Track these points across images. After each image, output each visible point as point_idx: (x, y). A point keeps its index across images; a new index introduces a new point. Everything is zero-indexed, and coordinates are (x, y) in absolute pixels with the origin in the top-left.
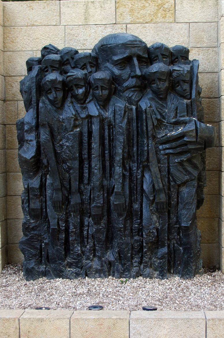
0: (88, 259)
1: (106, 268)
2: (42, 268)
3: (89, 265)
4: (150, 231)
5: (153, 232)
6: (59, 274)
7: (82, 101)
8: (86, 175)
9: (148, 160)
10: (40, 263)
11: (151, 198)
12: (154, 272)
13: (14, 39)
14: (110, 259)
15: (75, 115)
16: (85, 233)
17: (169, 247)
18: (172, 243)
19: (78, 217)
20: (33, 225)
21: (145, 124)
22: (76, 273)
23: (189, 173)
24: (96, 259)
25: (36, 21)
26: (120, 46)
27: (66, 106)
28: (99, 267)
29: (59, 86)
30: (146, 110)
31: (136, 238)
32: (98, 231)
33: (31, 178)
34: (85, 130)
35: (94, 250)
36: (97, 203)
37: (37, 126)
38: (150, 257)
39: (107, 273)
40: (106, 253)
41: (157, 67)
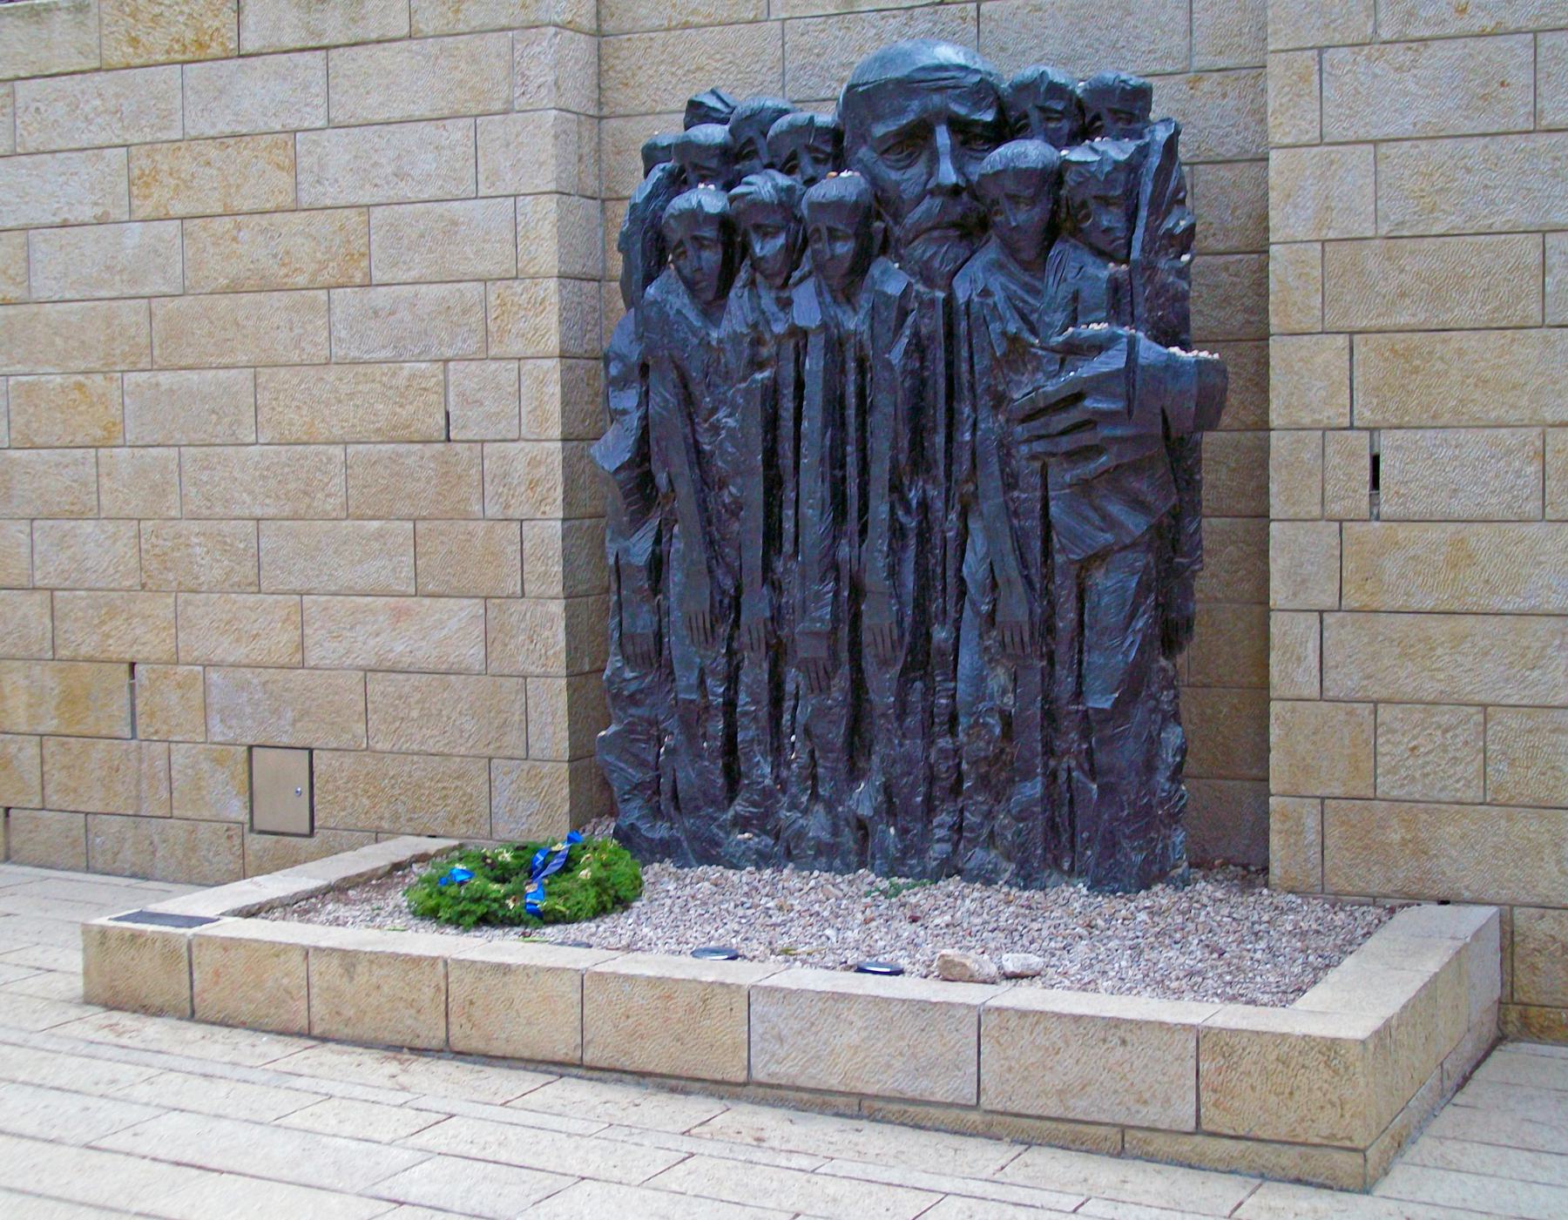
0: (793, 806)
1: (848, 839)
2: (661, 831)
3: (796, 826)
4: (976, 721)
5: (985, 725)
7: (783, 277)
8: (789, 526)
11: (984, 608)
12: (1004, 864)
13: (629, 74)
14: (860, 812)
15: (755, 326)
18: (1065, 766)
19: (765, 666)
20: (633, 687)
21: (965, 353)
22: (758, 852)
23: (1110, 523)
24: (819, 808)
25: (694, 12)
26: (890, 87)
27: (732, 294)
28: (825, 836)
29: (709, 232)
30: (968, 303)
31: (944, 742)
32: (820, 712)
33: (623, 533)
34: (789, 371)
35: (814, 777)
36: (814, 620)
37: (644, 369)
38: (990, 812)
39: (853, 858)
40: (852, 790)
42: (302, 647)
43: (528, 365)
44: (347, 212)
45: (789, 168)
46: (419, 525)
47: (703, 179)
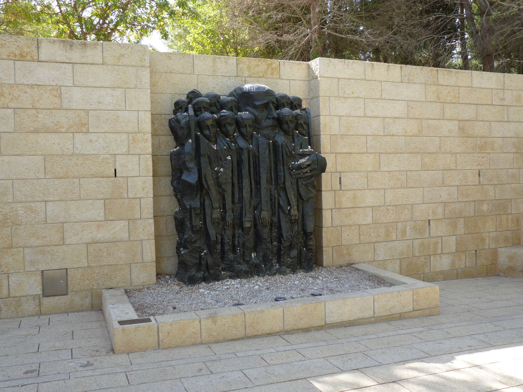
0: (239, 263)
6: (217, 278)
9: (284, 183)
10: (199, 270)
16: (236, 242)
17: (297, 248)
29: (215, 124)
41: (286, 110)
42: (63, 239)
43: (142, 156)
44: (80, 111)
45: (231, 109)
46: (106, 201)
47: (206, 111)
